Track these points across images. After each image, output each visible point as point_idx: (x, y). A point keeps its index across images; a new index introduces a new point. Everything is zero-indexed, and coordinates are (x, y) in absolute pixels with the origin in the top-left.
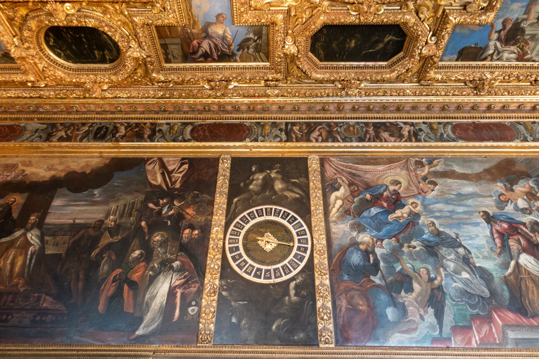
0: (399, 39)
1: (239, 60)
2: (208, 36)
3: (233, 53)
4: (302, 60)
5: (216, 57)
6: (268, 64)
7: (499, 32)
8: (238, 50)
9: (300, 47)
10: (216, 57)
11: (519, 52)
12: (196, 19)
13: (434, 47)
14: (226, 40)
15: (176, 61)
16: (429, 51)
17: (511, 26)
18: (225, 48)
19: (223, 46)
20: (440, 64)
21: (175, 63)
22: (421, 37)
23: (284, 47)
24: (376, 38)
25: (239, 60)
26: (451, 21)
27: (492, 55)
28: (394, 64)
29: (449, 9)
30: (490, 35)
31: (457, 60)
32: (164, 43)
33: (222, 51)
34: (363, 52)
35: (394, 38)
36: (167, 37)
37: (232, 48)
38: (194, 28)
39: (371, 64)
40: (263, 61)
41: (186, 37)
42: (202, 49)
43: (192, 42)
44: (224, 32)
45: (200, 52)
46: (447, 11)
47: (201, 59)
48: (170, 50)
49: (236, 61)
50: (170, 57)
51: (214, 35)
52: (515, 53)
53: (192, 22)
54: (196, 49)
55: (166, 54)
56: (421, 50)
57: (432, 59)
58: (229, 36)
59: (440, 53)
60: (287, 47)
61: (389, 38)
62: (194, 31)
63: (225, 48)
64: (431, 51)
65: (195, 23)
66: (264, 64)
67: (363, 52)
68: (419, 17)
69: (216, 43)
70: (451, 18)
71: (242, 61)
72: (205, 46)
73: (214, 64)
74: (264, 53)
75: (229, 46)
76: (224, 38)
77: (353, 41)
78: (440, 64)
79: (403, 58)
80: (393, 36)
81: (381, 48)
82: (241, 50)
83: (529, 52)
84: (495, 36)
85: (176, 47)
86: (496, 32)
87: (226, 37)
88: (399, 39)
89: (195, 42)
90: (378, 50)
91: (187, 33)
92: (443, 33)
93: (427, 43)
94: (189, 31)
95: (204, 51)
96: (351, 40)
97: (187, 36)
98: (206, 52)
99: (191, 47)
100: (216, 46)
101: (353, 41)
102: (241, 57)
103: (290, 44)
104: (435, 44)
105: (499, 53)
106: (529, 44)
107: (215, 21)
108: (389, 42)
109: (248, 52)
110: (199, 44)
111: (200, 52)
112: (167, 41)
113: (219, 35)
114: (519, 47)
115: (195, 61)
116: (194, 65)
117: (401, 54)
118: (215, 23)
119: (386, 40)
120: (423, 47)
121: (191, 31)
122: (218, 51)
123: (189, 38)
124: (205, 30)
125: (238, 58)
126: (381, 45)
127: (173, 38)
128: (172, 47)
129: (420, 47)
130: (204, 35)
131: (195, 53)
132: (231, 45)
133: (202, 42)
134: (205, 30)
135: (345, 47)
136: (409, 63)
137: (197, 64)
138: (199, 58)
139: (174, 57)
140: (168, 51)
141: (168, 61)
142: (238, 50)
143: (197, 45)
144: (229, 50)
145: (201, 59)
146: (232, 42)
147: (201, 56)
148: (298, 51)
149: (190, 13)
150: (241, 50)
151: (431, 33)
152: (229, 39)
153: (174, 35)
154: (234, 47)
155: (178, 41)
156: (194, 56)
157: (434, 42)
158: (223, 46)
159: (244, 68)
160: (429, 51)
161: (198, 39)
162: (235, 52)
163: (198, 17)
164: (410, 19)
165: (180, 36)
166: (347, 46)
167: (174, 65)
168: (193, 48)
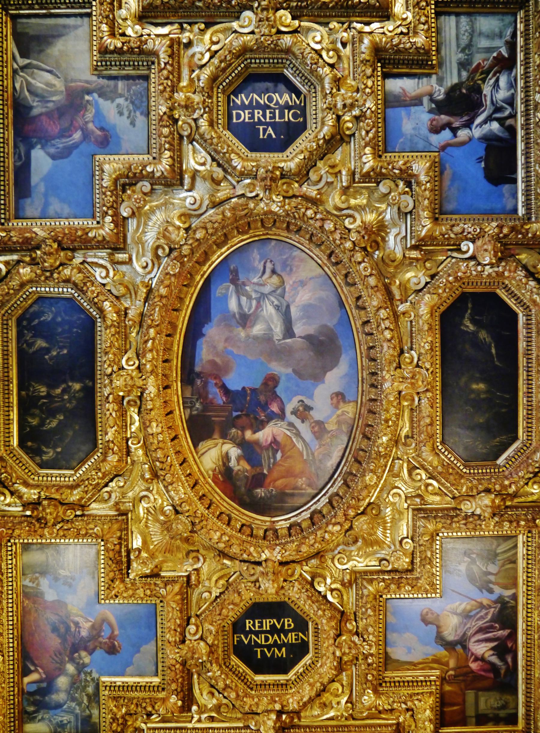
0: (470, 305)
1: (513, 591)
2: (463, 642)
3: (496, 602)
4: (507, 483)
5: (506, 632)
6: (520, 537)
7: (454, 131)
8: (491, 591)
9: (481, 488)
10: (506, 632)
11: (494, 75)
12: (431, 658)
13: (479, 243)
14: (470, 611)
15: (512, 705)
16: (486, 250)
17: (443, 116)
18: (487, 614)
19: (482, 618)
20: (521, 211)
21: (517, 708)
22: (459, 274)
23: (479, 516)
24: (467, 346)
25: (513, 591)
26: (429, 230)
27: (501, 121)
28: (519, 301)
29: (411, 239)
30: (462, 144)
31: (515, 181)
32: (474, 720)
33: (491, 621)
34: (497, 363)
35: (467, 315)
36: (463, 711)
37: (485, 602)
38: (447, 664)
39: (522, 345)
40: (516, 546)
41: (464, 681)
42: (486, 655)
43: (472, 672)
44: (456, 614)
45: (494, 659)
46: (413, 243)
47: (509, 660)
48: (489, 712)
49: (515, 597)
50: (502, 713)
51: (460, 632)
52: (497, 80)
53: (435, 666)
54: (487, 667)
55: (497, 720)
56: (486, 265)
57: (506, 236)
58: (463, 606)
59: (491, 228)
60: (478, 512)
61: (468, 323)
62: (452, 663)
63: (487, 614)
64: (485, 247)
65: (437, 661)
66: (520, 545)
67: (497, 363)
68: (424, 287)
69: (475, 629)
70: (423, 233)
71: (515, 585)
72: (482, 649)
73: (521, 638)
74: (498, 545)
75: (482, 606)
76: (467, 616)
77: (474, 386)
78: (521, 211)
79: (506, 288)
80: (463, 317)
81: (488, 332)
82: (491, 586)
83: (495, 54)
84: (463, 134)
85: (482, 700)
86: (455, 136)
87: (464, 610)
88: (470, 305)
89: (474, 666)
90: (492, 338)
91: (455, 676)
92: (452, 236)
93: (473, 258)
94: (451, 673)
95: (491, 652)
96: (473, 391)
97: (461, 678)
98: (493, 649)
99: (483, 673)
100: (481, 630)
101: (474, 386)
102: (506, 588)
103: (474, 504)
104: (473, 242)
105: (498, 109)
106: (479, 64)
107: (435, 627)
108: (473, 321)
109: (496, 575)
110: (476, 659)
111: (494, 659)
112: (470, 712)
113: (460, 624)
114: (484, 80)
115: (513, 671)
116: (521, 675)
117: (502, 294)
118: (438, 627)
119: (472, 328)
120: (479, 264)
121: (452, 669)
122: (492, 627)
123: (465, 674)
124: (450, 646)
125: (508, 593)
126: (483, 335)
127: (464, 701)
128: (482, 705)
129: (479, 268)
130: (459, 648)
131: (493, 668)
132: (481, 603)
133: (473, 654)
134: (450, 646)
135: (484, 399)
136: (514, 278)
137: (520, 668)
138: (506, 663)
139: (504, 707)
140: (491, 715)
141: (512, 720)
142: (491, 591)
143: (480, 663)
144: (490, 607)
145: (509, 660)
146: (473, 602)
147: (502, 657)
148: (488, 491)
149: (421, 666)
150: (491, 586)
151: (455, 254)
152: (469, 607)
153: (460, 700)
154: (485, 599)
155: (470, 695)
156: (502, 672)
157: (471, 245)
158: (482, 618)
159: (527, 583)
160: (486, 250)
161: (467, 660)
162: (494, 597)
163: (427, 655)
164: (427, 302)
165: (461, 690)
166: (483, 396)
167: (521, 711)
168: (484, 670)
